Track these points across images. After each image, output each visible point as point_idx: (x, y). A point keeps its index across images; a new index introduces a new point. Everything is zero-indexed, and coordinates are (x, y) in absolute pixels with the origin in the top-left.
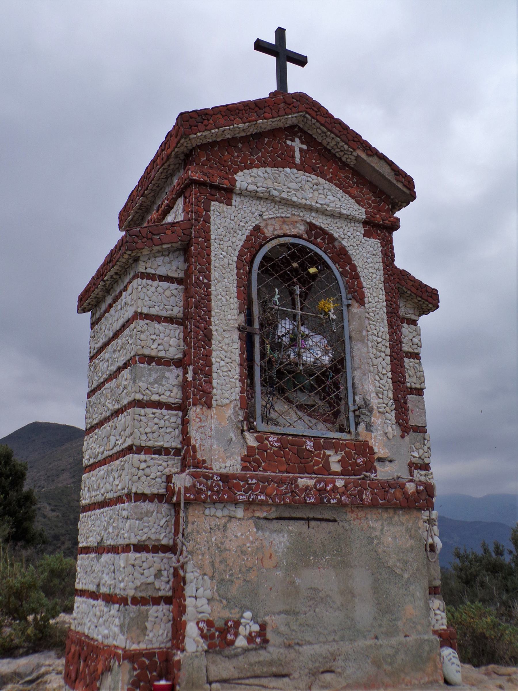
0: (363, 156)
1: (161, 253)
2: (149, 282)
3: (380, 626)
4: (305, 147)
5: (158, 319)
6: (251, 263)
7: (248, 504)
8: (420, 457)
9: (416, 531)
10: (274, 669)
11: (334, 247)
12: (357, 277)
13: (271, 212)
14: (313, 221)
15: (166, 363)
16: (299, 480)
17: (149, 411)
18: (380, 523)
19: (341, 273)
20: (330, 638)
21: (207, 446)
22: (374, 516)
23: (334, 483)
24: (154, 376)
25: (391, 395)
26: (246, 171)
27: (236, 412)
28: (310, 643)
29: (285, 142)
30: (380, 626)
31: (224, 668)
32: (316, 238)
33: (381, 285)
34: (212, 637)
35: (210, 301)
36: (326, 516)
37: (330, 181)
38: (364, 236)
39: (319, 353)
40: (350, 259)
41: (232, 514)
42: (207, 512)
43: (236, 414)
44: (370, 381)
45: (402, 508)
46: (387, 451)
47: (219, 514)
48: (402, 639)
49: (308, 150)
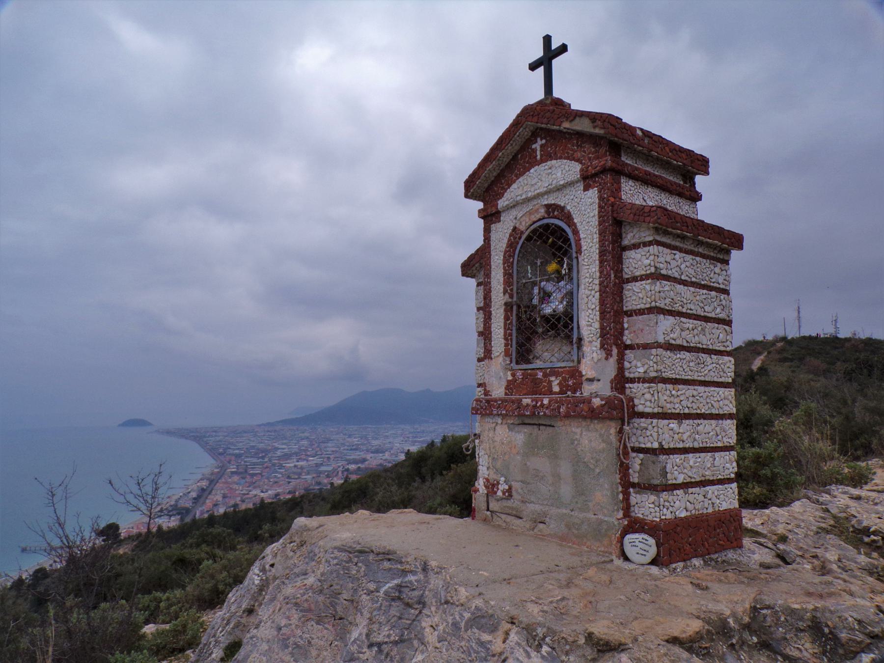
7: (504, 417)
8: (645, 372)
20: (545, 503)
28: (532, 502)
33: (596, 230)
37: (561, 158)
43: (504, 361)
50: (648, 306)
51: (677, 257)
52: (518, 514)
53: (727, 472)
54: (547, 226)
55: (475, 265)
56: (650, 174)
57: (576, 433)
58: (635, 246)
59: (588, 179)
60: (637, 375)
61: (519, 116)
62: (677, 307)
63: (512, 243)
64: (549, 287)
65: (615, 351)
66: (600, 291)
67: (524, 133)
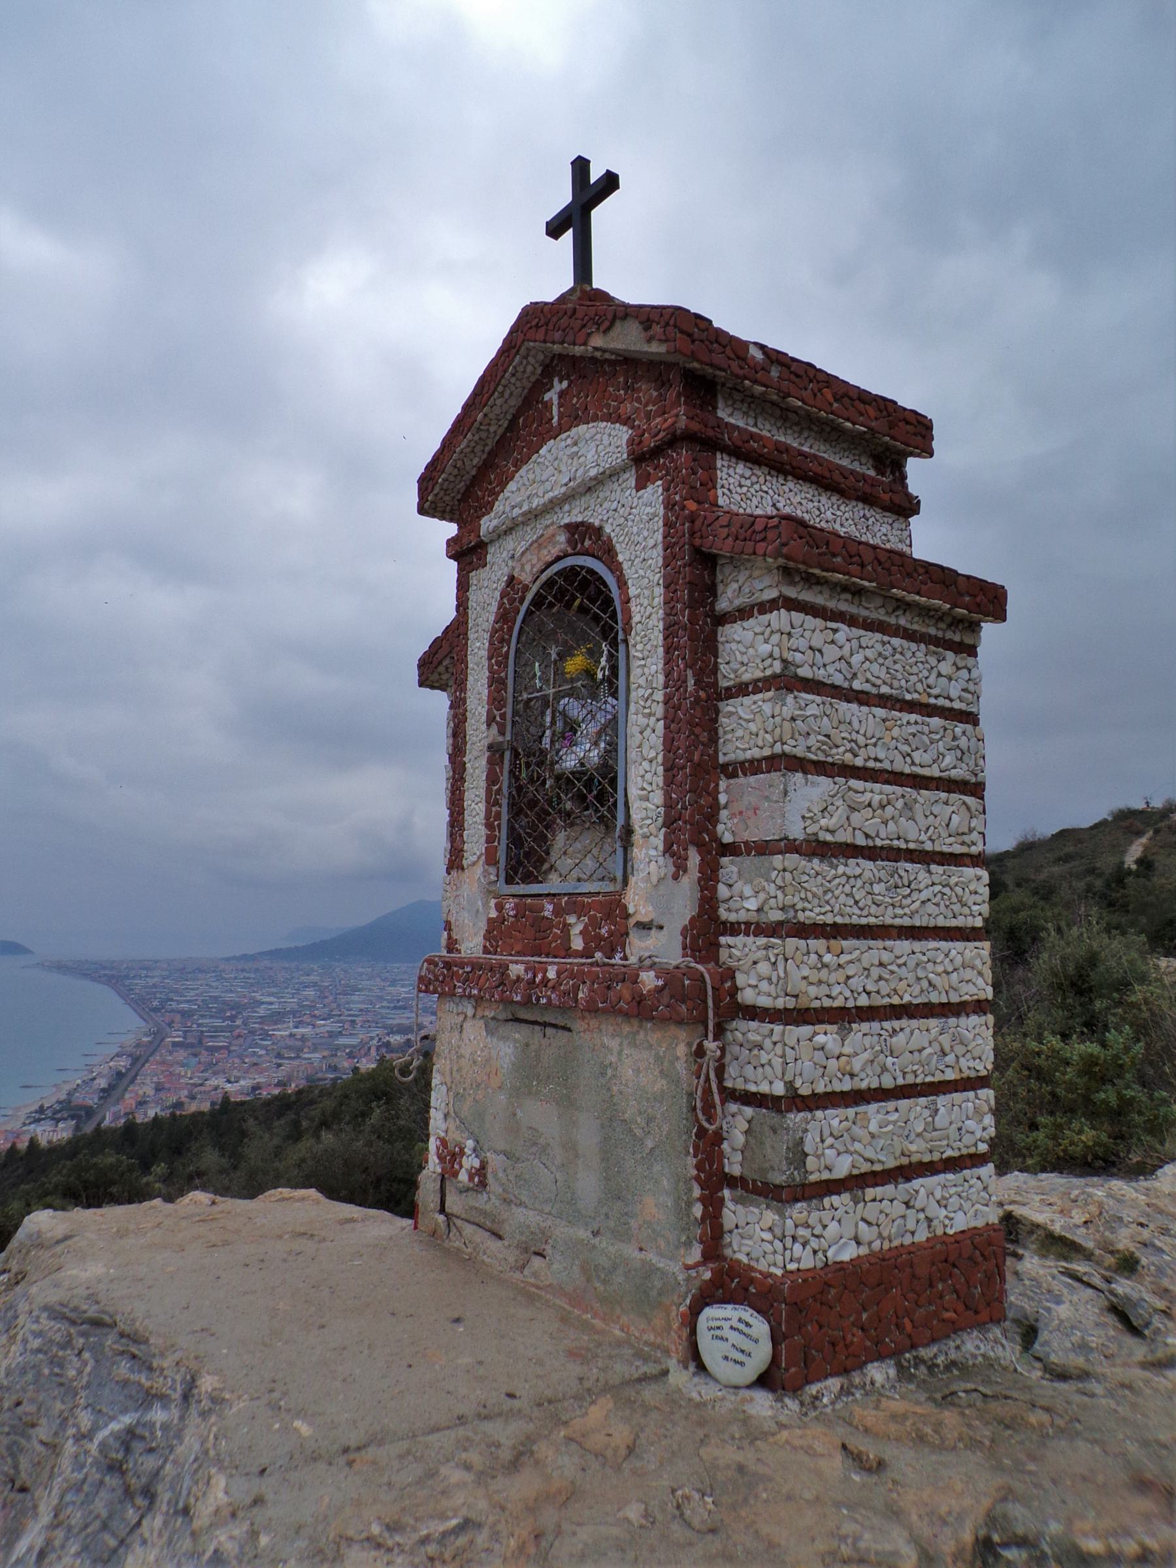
3: (607, 1216)
7: (478, 1001)
9: (672, 1063)
18: (617, 1040)
20: (547, 1209)
22: (611, 1028)
28: (521, 1204)
37: (595, 419)
43: (486, 873)
46: (651, 908)
50: (767, 752)
51: (841, 637)
52: (495, 1227)
53: (968, 1139)
54: (571, 573)
55: (441, 664)
56: (787, 449)
57: (610, 1050)
58: (743, 613)
59: (644, 460)
60: (742, 916)
61: (514, 330)
62: (839, 755)
64: (574, 708)
65: (694, 859)
66: (665, 718)
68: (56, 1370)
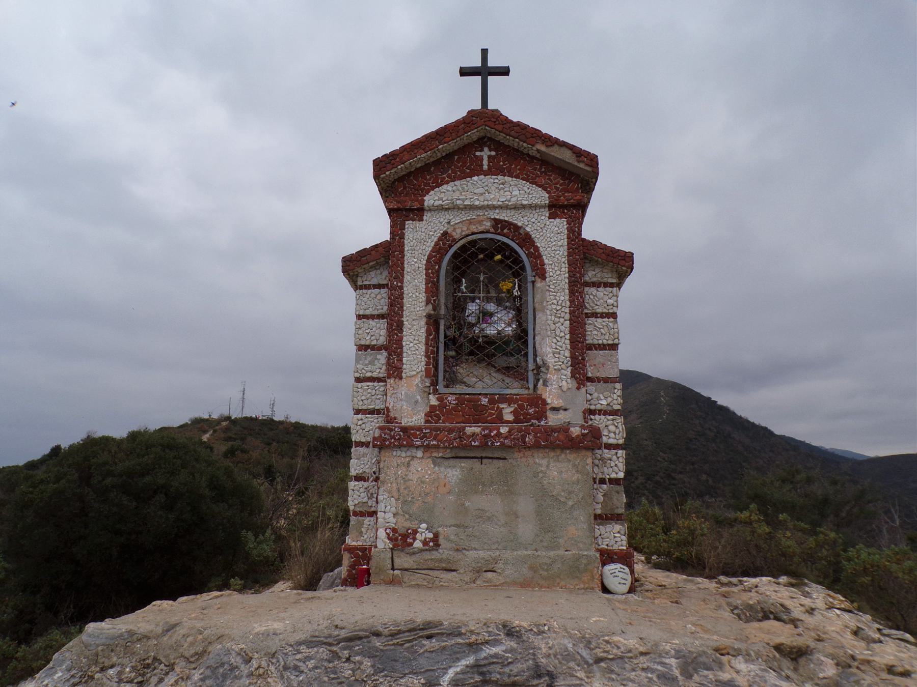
0: (543, 148)
1: (374, 268)
2: (365, 291)
4: (493, 153)
5: (372, 317)
6: (439, 262)
7: (427, 448)
10: (444, 565)
11: (520, 234)
12: (540, 256)
13: (456, 218)
14: (497, 217)
15: (379, 348)
16: (467, 429)
17: (364, 384)
18: (547, 460)
19: (527, 255)
21: (399, 406)
22: (541, 455)
23: (498, 430)
24: (369, 359)
25: (567, 354)
26: (437, 189)
27: (422, 380)
29: (474, 155)
30: (541, 541)
31: (403, 560)
32: (502, 230)
33: (565, 260)
34: (396, 539)
35: (403, 299)
36: (495, 456)
37: (517, 177)
38: (549, 218)
39: (503, 325)
40: (534, 242)
41: (414, 454)
42: (394, 453)
43: (423, 381)
44: (551, 344)
45: (568, 448)
47: (403, 454)
48: (561, 552)
49: (497, 155)
52: (449, 566)
57: (541, 465)
58: (596, 285)
60: (599, 407)
63: (440, 248)
67: (474, 134)
68: (332, 676)
